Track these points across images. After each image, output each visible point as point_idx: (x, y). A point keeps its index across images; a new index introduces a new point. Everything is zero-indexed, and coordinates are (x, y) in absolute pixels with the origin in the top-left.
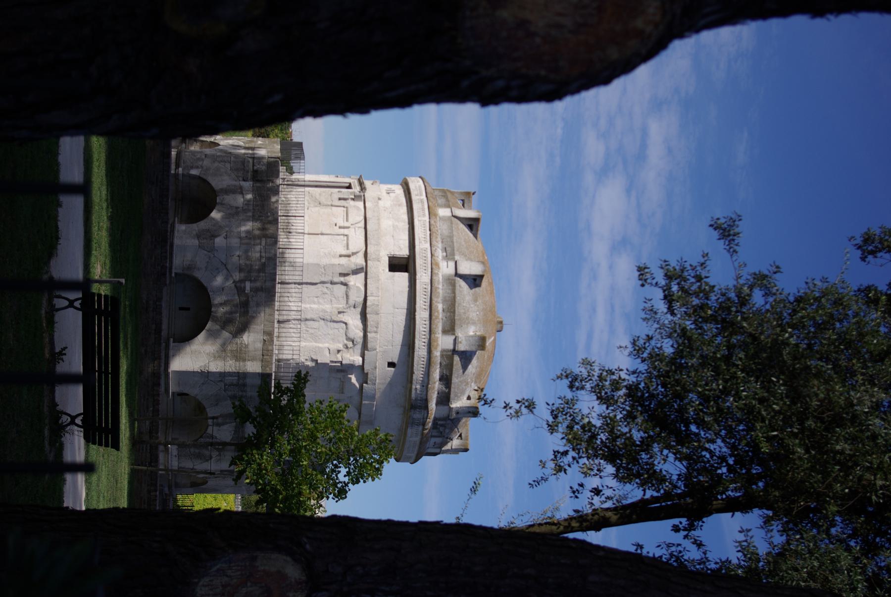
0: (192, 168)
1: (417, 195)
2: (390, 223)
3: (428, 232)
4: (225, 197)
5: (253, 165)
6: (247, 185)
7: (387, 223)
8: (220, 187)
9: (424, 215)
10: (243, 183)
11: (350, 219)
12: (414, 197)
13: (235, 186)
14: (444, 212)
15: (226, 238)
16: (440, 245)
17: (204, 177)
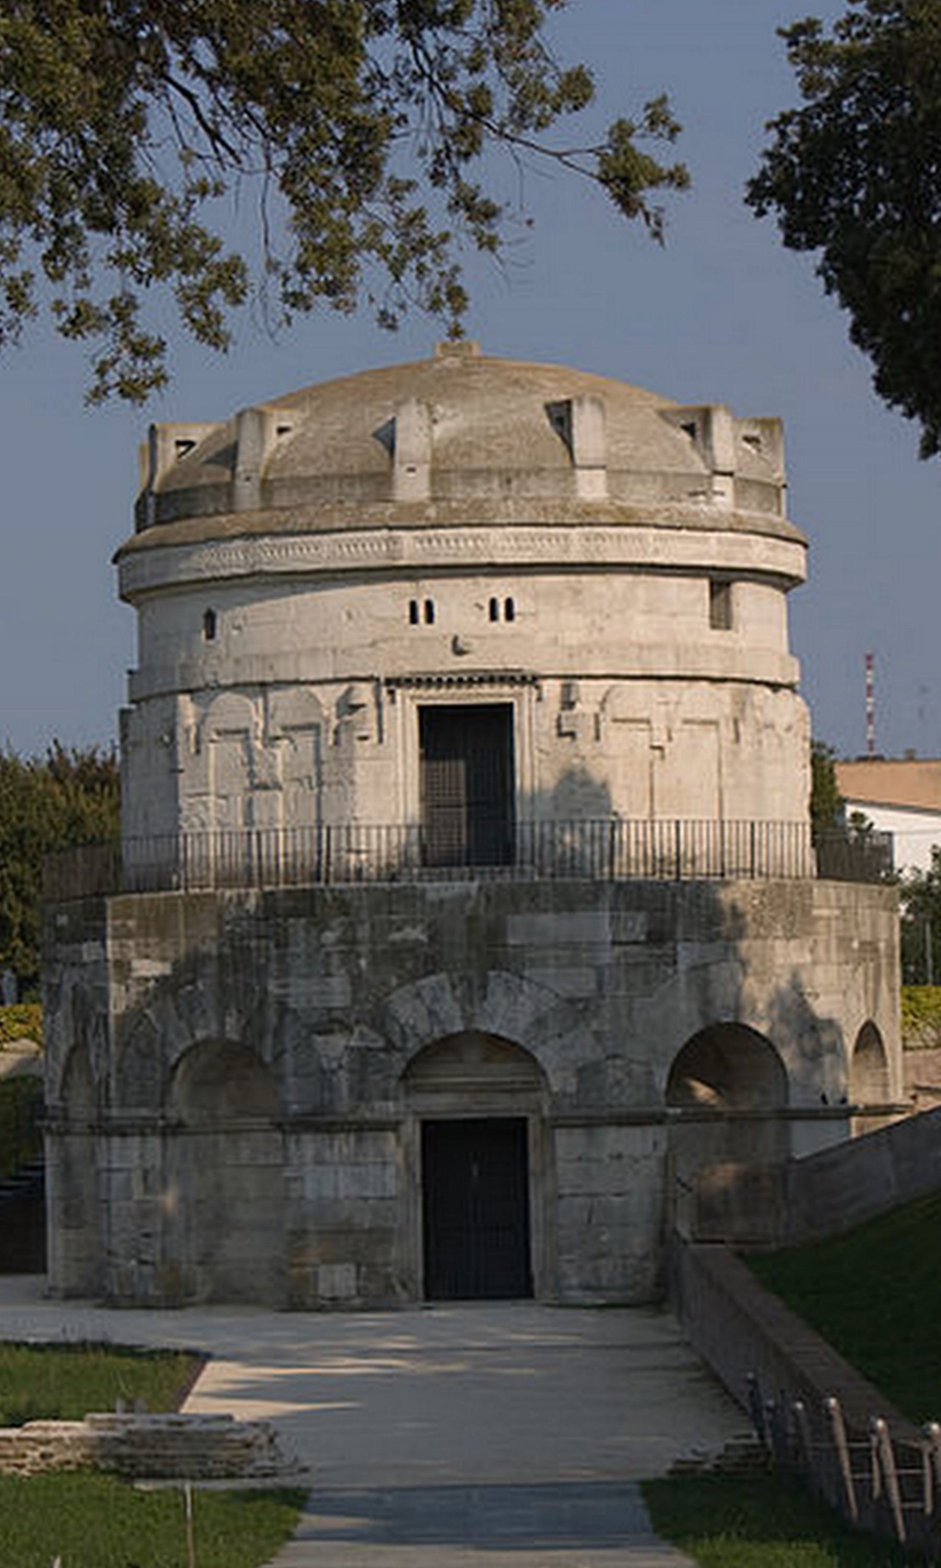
0: (651, 1087)
1: (566, 551)
2: (640, 619)
3: (684, 532)
4: (718, 1003)
5: (636, 943)
6: (686, 954)
7: (641, 627)
8: (695, 1017)
9: (640, 538)
10: (682, 967)
11: (644, 715)
12: (574, 556)
13: (689, 984)
14: (592, 488)
15: (817, 996)
16: (687, 506)
17: (672, 1055)
